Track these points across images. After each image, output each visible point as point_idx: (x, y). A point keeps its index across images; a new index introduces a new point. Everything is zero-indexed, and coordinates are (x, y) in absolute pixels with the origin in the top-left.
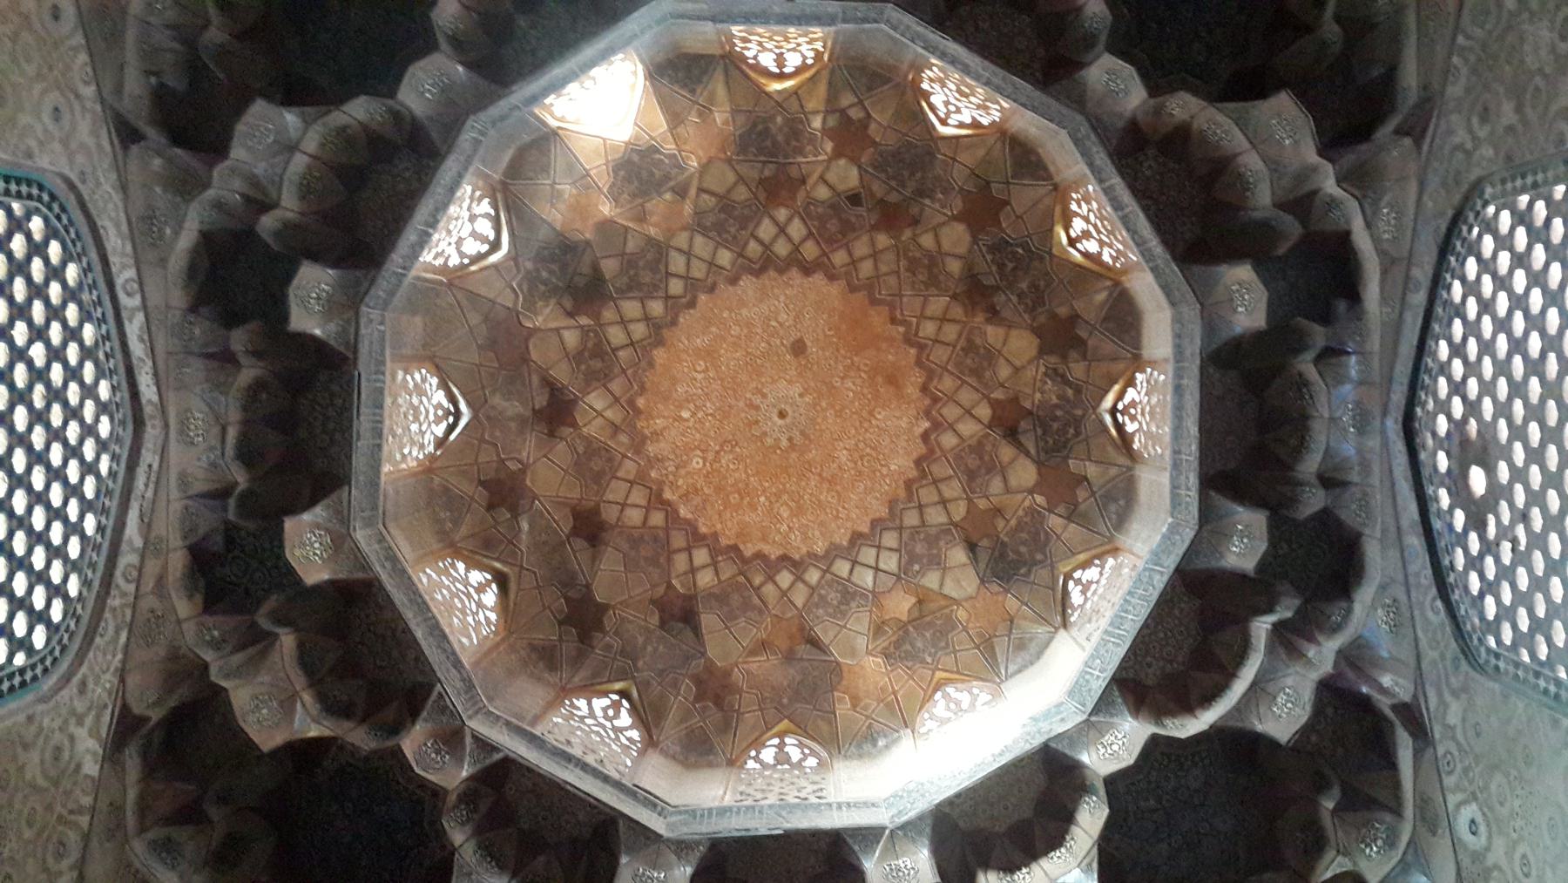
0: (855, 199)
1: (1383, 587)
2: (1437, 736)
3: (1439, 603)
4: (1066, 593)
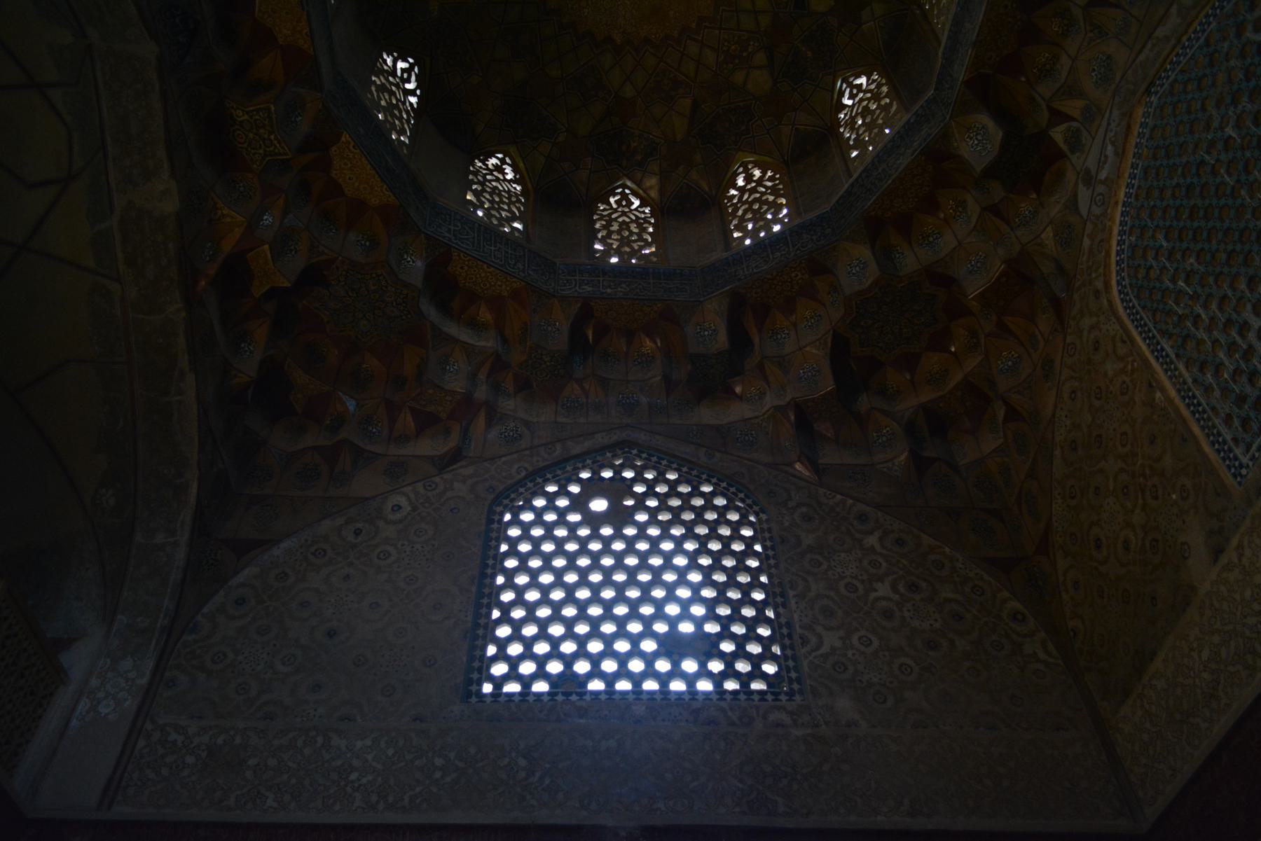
1: (527, 424)
2: (446, 476)
3: (524, 474)
4: (492, 155)
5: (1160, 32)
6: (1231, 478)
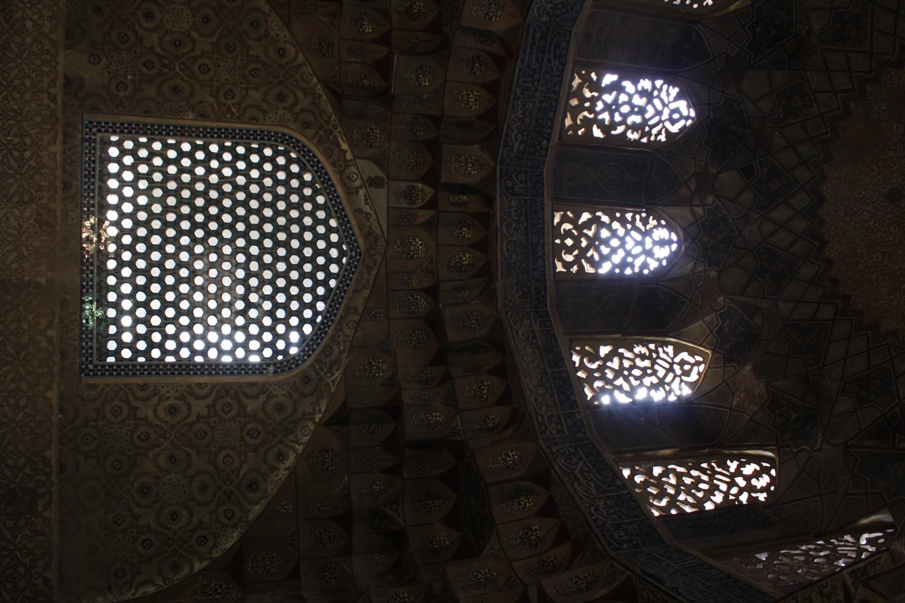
0: (748, 172)
5: (366, 292)
6: (100, 119)
